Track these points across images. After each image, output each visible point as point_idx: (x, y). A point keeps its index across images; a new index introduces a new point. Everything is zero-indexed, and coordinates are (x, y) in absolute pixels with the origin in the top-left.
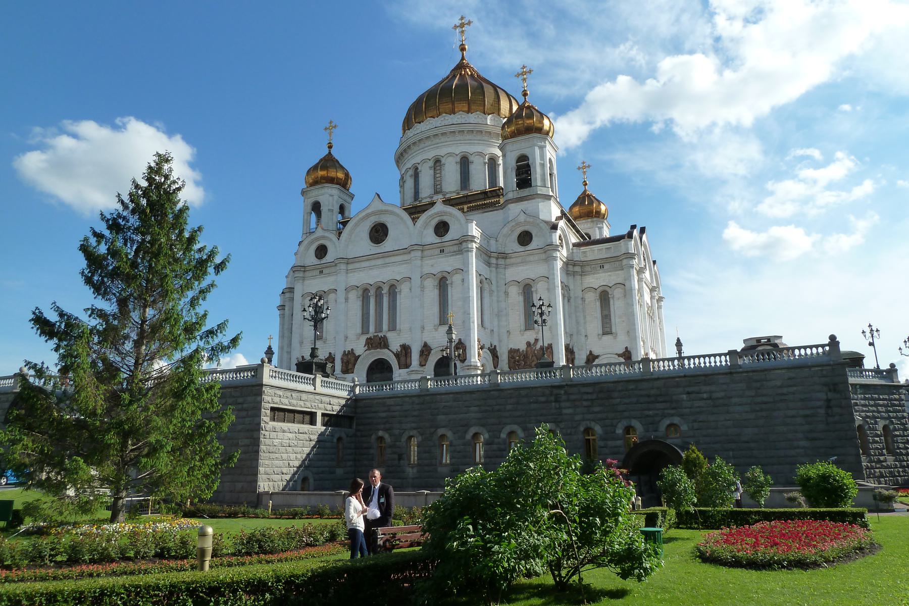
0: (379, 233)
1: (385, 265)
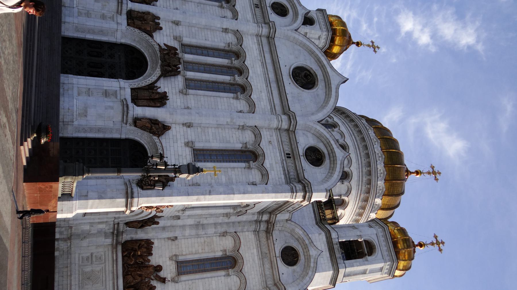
0: (304, 78)
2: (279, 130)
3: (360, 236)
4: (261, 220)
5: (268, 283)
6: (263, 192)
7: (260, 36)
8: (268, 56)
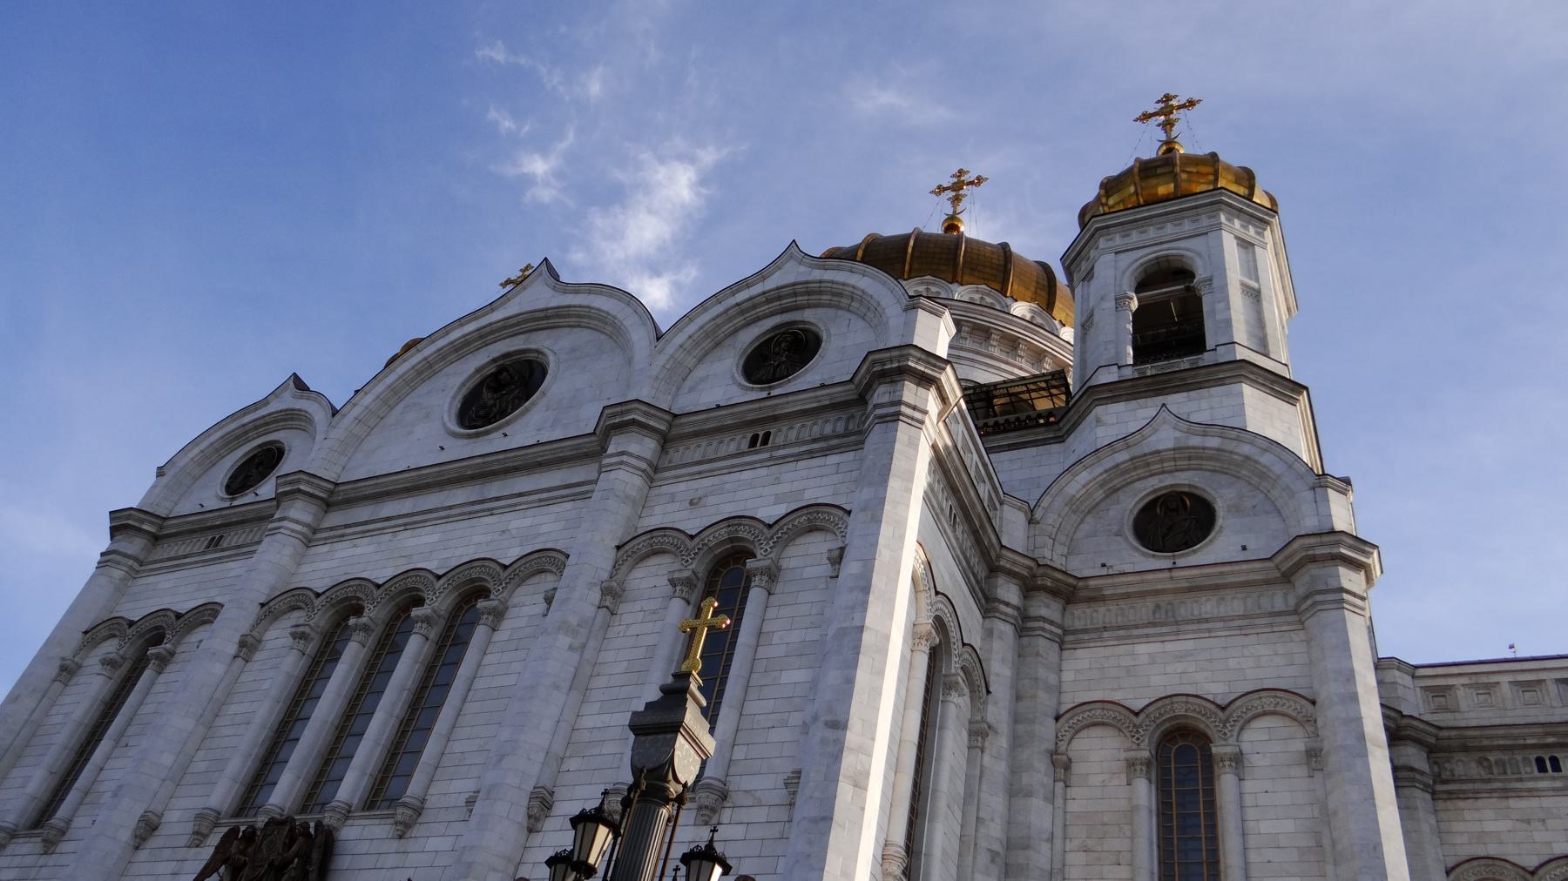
2: (656, 470)
3: (1121, 300)
4: (1017, 608)
5: (1279, 604)
6: (877, 520)
7: (315, 531)
8: (391, 508)
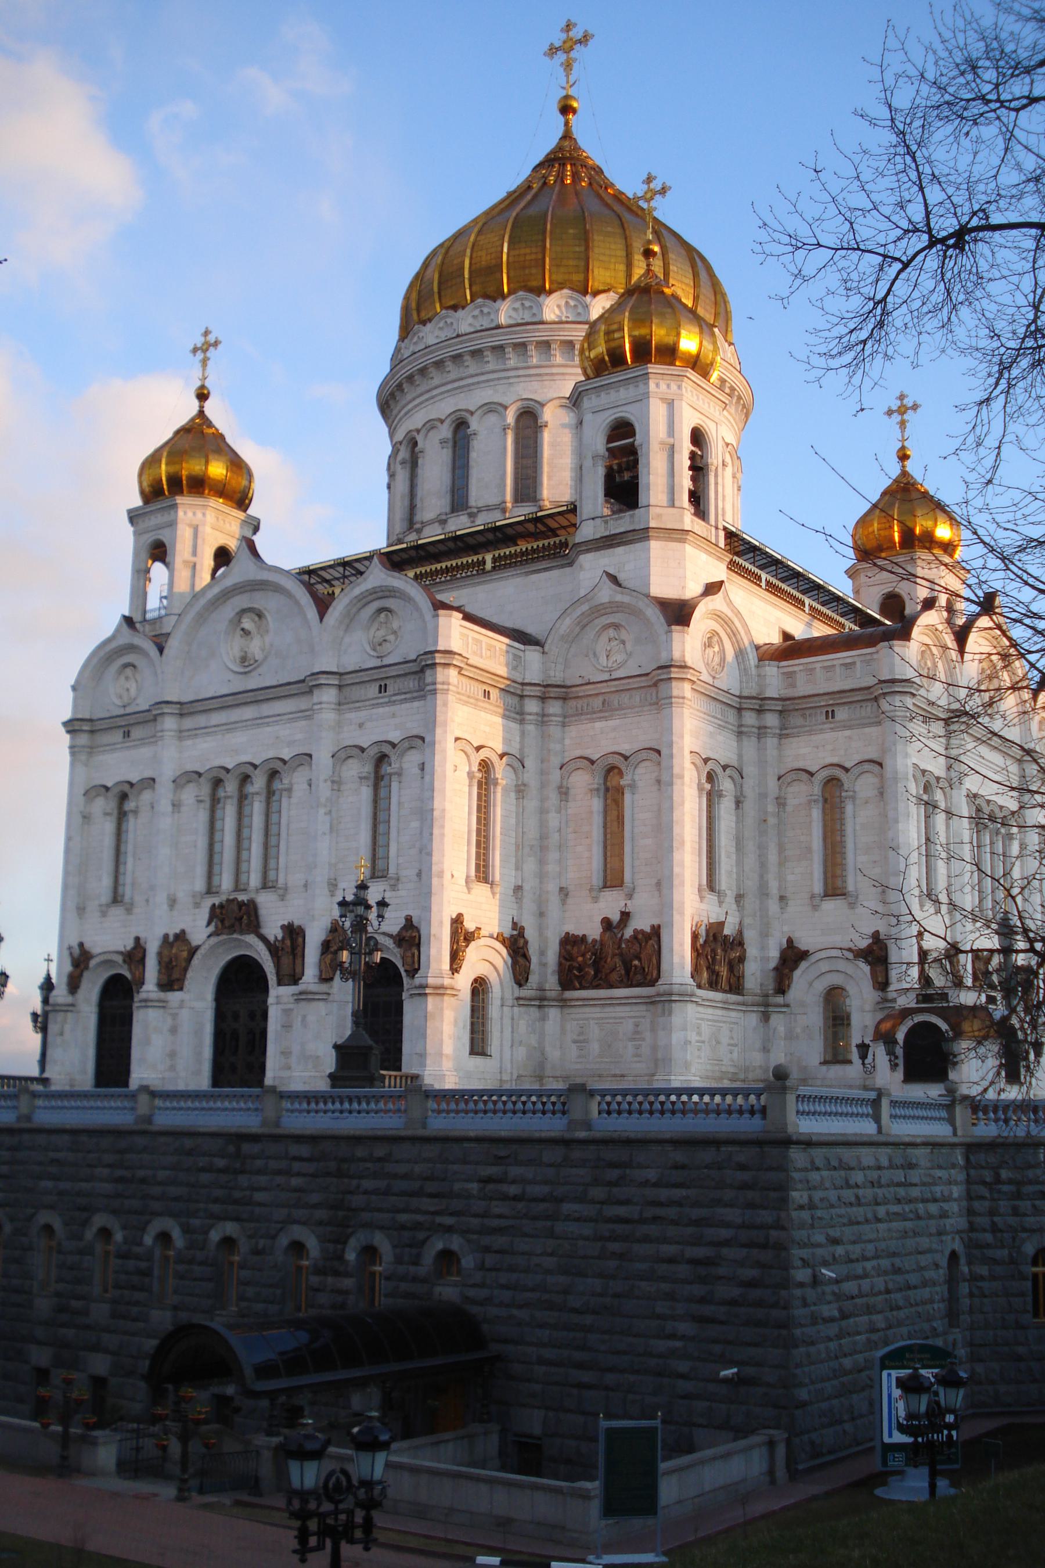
1: (260, 721)
8: (217, 718)
